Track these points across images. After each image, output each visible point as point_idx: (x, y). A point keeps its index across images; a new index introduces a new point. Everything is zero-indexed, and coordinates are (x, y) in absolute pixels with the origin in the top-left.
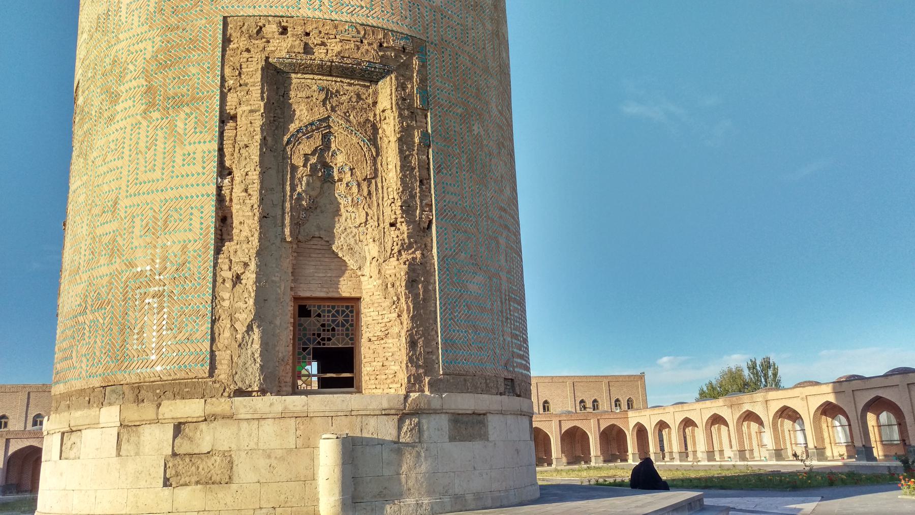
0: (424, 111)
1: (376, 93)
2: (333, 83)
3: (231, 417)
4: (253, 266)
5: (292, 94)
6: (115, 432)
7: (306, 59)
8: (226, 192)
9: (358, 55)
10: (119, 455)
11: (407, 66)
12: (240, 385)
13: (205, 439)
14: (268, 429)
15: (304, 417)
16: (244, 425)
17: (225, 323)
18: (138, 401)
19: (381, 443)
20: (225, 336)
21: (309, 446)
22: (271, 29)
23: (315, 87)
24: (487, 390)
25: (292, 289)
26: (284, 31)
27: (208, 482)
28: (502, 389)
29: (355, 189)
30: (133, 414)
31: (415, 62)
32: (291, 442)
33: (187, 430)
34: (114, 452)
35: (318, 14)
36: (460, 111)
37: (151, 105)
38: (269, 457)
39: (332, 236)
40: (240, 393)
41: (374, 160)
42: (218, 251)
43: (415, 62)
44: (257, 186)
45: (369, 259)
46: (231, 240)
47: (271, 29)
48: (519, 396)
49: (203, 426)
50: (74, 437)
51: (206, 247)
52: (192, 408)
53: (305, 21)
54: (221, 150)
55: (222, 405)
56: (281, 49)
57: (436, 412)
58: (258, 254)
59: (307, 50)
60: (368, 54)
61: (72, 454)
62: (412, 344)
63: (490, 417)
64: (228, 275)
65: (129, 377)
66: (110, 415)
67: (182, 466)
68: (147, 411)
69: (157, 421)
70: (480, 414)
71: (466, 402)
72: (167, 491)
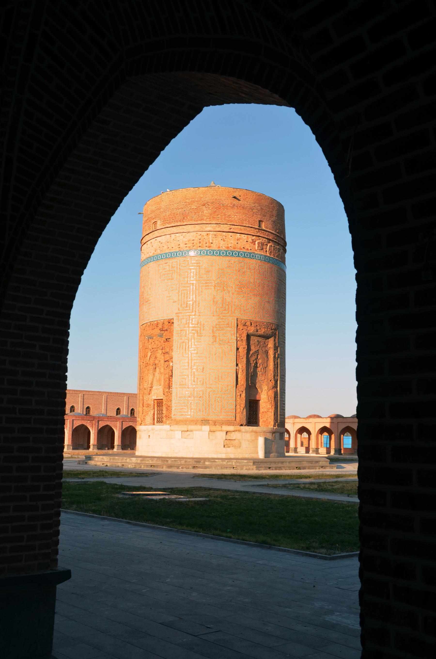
0: (278, 347)
1: (268, 342)
2: (260, 339)
4: (244, 392)
5: (251, 342)
6: (207, 433)
7: (257, 333)
8: (237, 371)
9: (267, 332)
10: (209, 438)
11: (275, 334)
12: (242, 423)
13: (233, 436)
15: (256, 432)
16: (243, 433)
17: (238, 407)
19: (269, 439)
20: (238, 410)
21: (257, 439)
22: (248, 323)
23: (256, 340)
27: (235, 446)
29: (263, 370)
30: (214, 428)
31: (277, 332)
32: (253, 438)
33: (228, 433)
34: (208, 438)
35: (260, 320)
39: (256, 383)
40: (242, 425)
41: (267, 361)
43: (277, 332)
44: (245, 370)
45: (264, 390)
49: (233, 433)
52: (231, 428)
53: (256, 322)
55: (239, 427)
56: (252, 330)
58: (246, 389)
59: (257, 331)
60: (270, 332)
62: (274, 414)
64: (239, 394)
66: (206, 428)
67: (228, 442)
68: (218, 427)
72: (225, 449)
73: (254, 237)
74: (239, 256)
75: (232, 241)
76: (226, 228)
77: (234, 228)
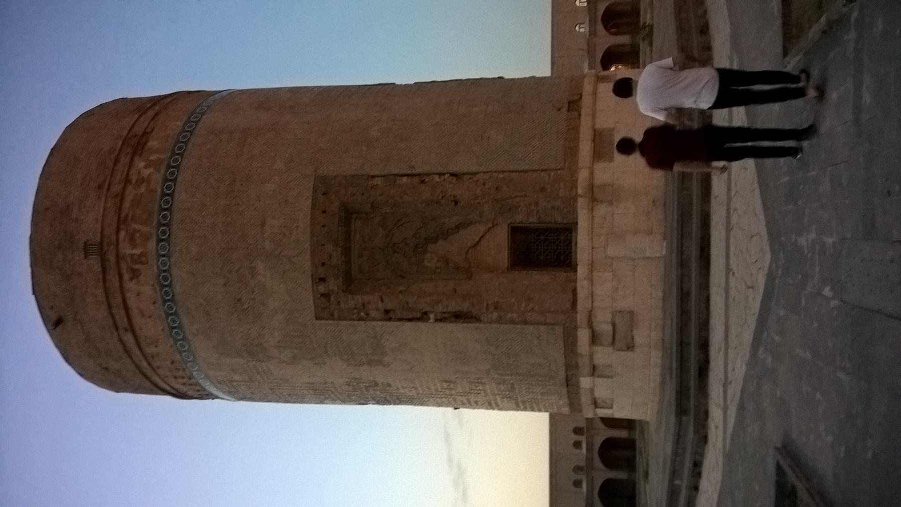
3: (590, 312)
6: (597, 380)
13: (604, 328)
14: (599, 290)
16: (596, 304)
18: (577, 366)
22: (322, 288)
24: (576, 129)
25: (503, 272)
26: (322, 280)
28: (576, 114)
30: (585, 368)
34: (610, 380)
35: (308, 257)
36: (364, 148)
37: (380, 362)
38: (617, 289)
42: (478, 320)
46: (471, 312)
47: (322, 288)
48: (581, 95)
50: (599, 401)
51: (477, 328)
52: (583, 336)
54: (410, 320)
55: (581, 317)
57: (592, 173)
61: (609, 402)
63: (597, 126)
65: (562, 374)
66: (585, 382)
68: (584, 362)
69: (591, 356)
70: (595, 136)
71: (585, 149)
73: (124, 271)
74: (175, 314)
75: (151, 328)
76: (129, 339)
77: (123, 322)
